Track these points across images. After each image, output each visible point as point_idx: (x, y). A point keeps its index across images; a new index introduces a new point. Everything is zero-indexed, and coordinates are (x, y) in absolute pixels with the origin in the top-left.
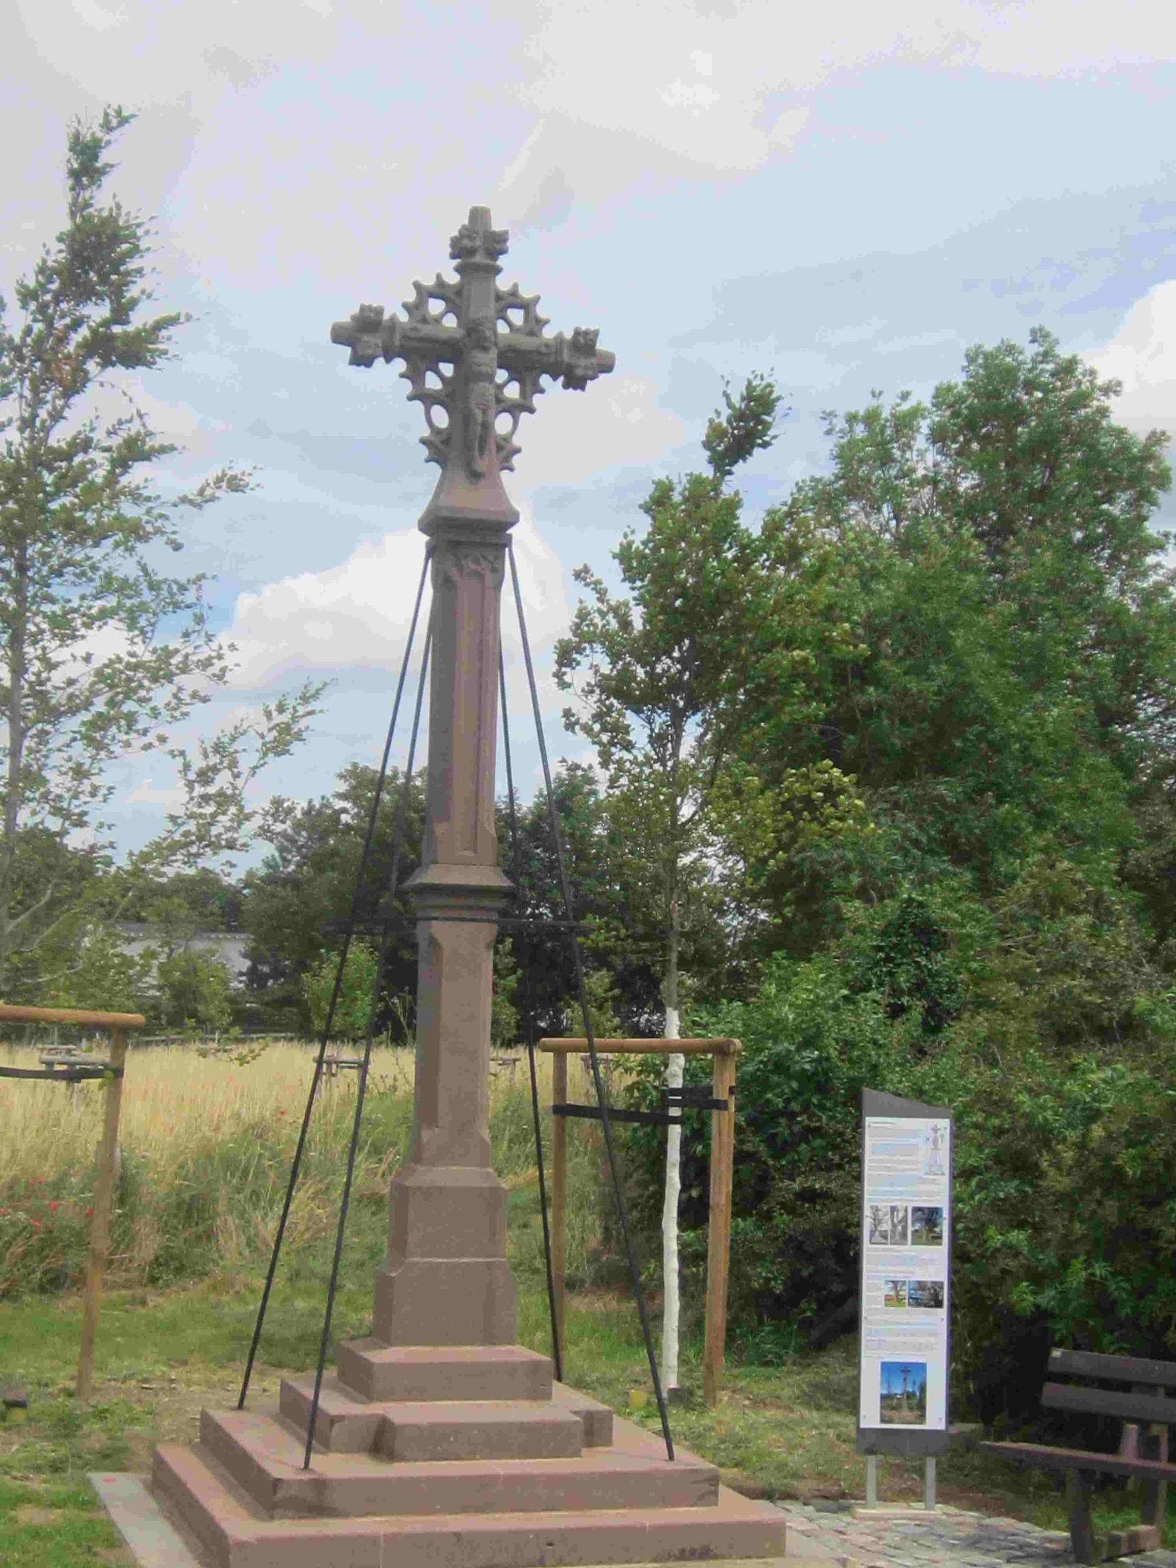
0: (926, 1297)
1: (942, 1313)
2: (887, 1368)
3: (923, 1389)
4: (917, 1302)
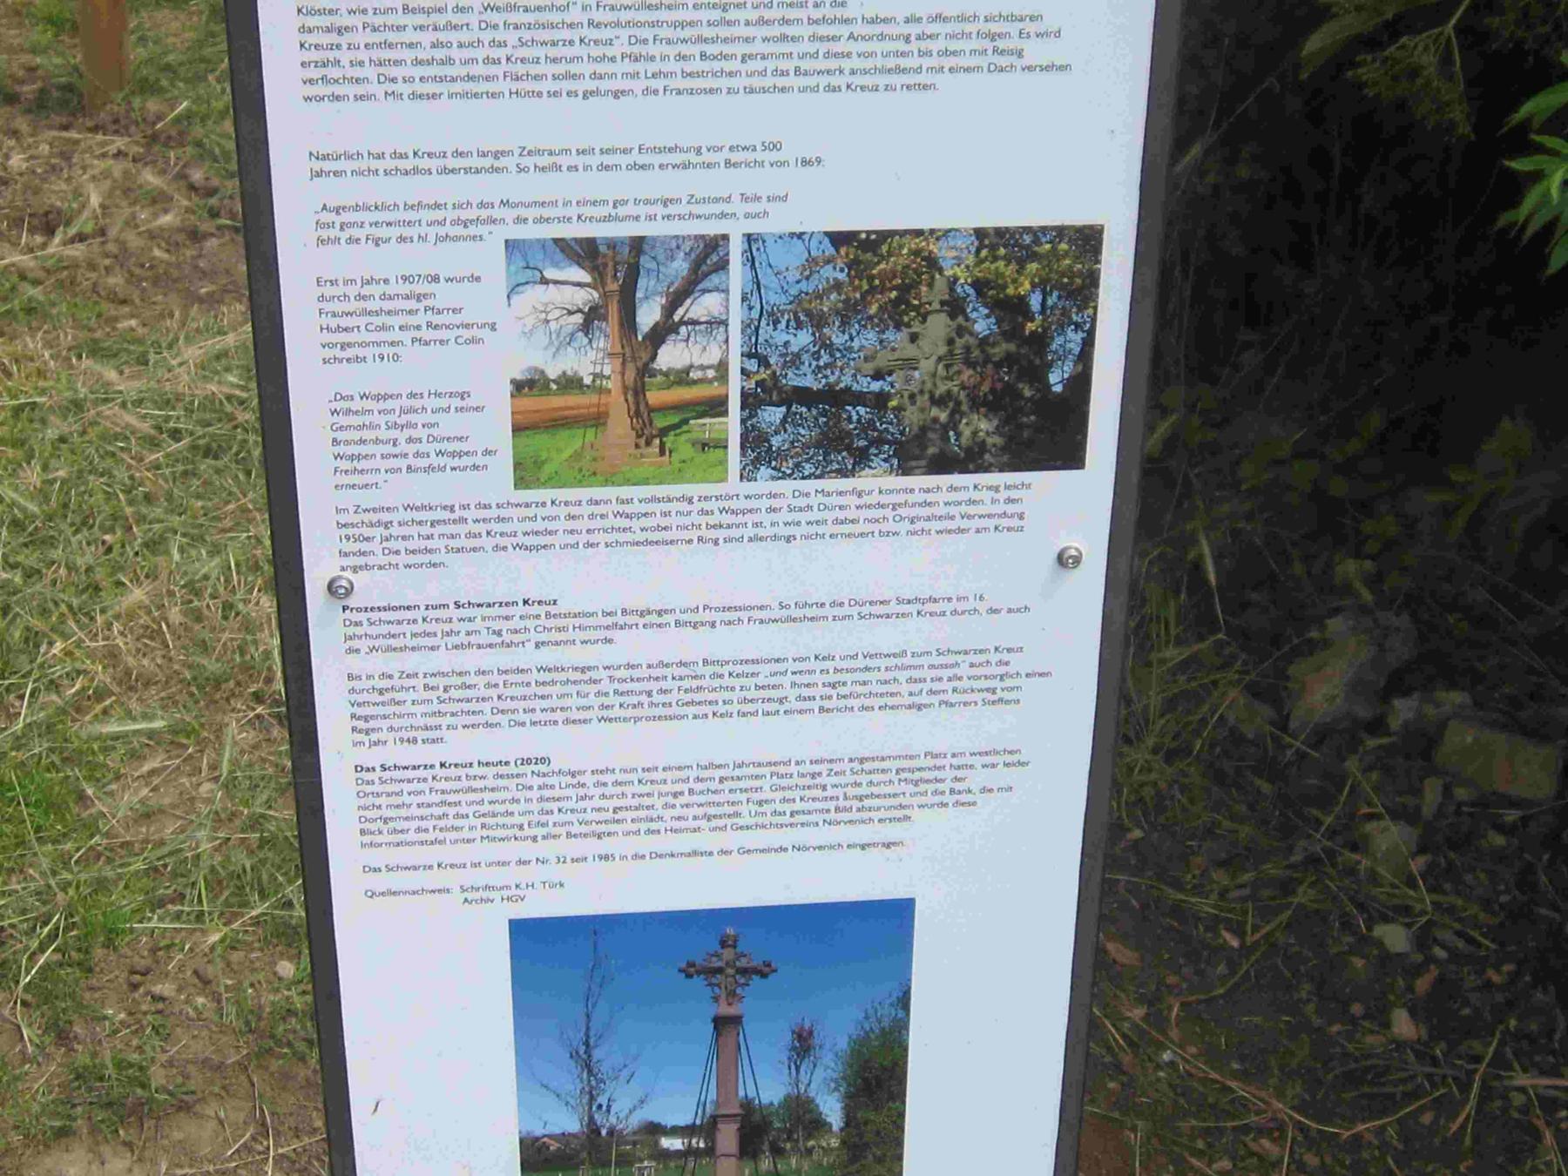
0: (915, 362)
1: (1076, 505)
2: (567, 966)
3: (878, 1078)
4: (827, 427)
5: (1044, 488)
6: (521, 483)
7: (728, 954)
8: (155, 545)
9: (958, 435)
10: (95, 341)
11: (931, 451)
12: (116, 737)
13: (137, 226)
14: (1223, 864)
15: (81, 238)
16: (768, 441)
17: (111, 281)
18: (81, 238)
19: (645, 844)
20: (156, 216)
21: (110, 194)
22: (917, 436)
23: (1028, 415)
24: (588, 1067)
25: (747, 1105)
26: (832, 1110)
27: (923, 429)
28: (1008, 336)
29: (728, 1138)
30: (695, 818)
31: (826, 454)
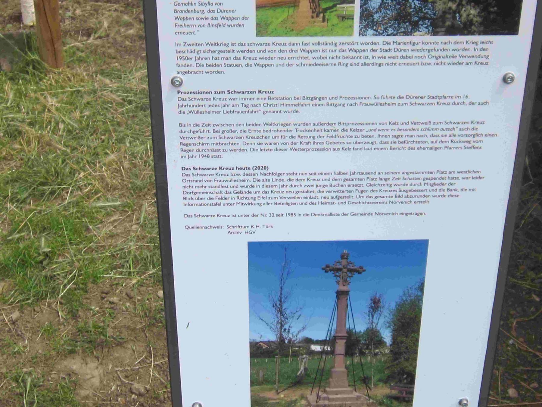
3: (408, 323)
5: (500, 42)
6: (259, 33)
7: (344, 262)
8: (121, 141)
9: (461, 16)
10: (102, 70)
11: (448, 23)
12: (101, 207)
13: (121, 34)
14: (533, 269)
15: (100, 37)
16: (372, 16)
17: (110, 51)
18: (100, 37)
19: (309, 209)
20: (127, 30)
21: (111, 23)
22: (441, 17)
23: (493, 7)
24: (281, 312)
25: (350, 333)
26: (387, 336)
27: (444, 13)
29: (340, 347)
30: (332, 198)
31: (399, 24)
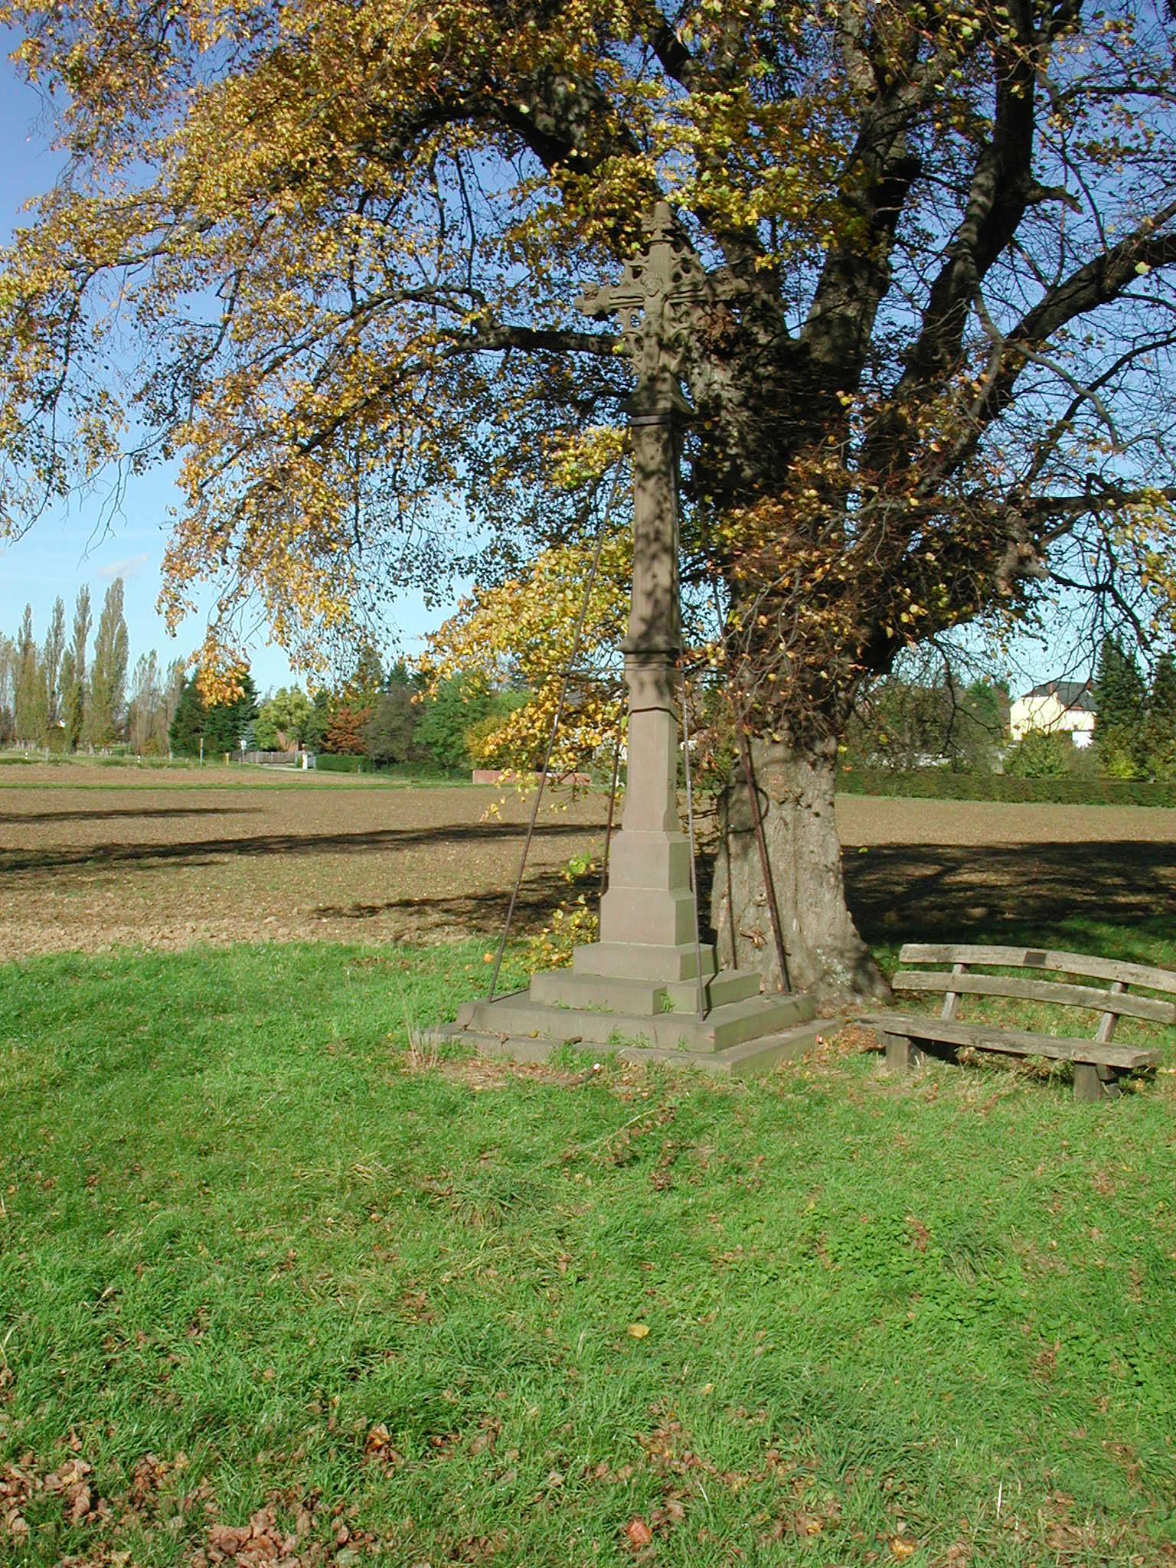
11: (663, 404)
16: (487, 389)
22: (645, 388)
23: (765, 365)
27: (652, 379)
28: (740, 269)
